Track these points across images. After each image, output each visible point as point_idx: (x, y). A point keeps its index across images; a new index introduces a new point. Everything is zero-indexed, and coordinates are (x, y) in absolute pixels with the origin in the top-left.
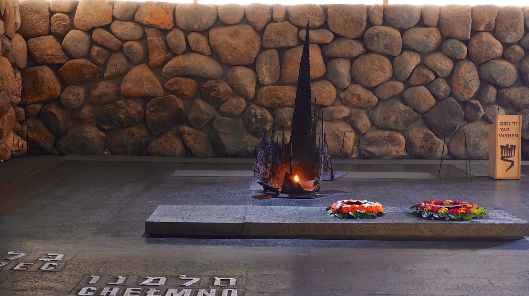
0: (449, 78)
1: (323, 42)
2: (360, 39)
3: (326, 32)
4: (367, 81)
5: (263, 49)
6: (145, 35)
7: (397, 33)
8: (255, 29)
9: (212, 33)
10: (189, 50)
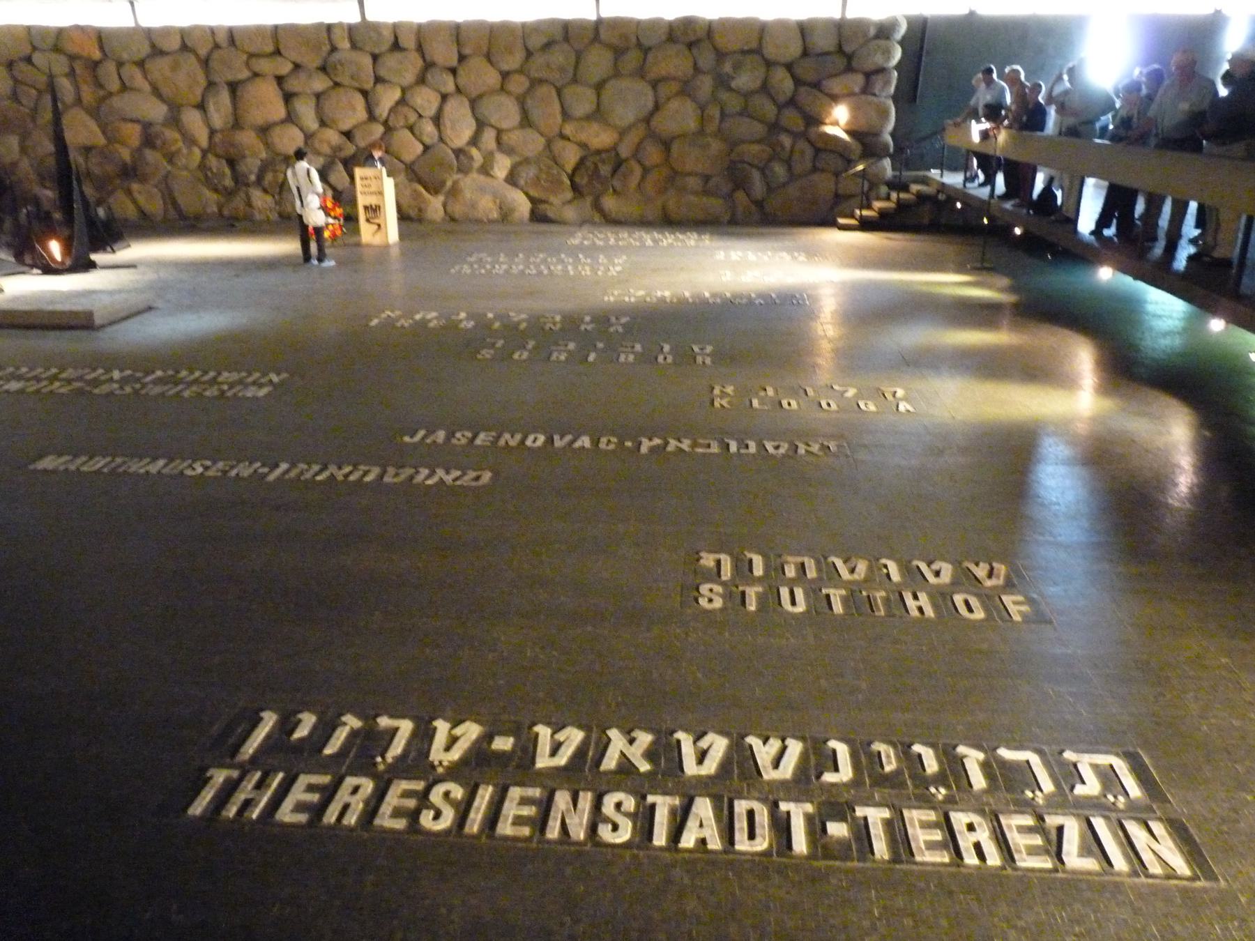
0: (437, 120)
2: (323, 69)
3: (279, 59)
5: (211, 84)
6: (73, 70)
7: (367, 61)
8: (197, 56)
10: (124, 88)
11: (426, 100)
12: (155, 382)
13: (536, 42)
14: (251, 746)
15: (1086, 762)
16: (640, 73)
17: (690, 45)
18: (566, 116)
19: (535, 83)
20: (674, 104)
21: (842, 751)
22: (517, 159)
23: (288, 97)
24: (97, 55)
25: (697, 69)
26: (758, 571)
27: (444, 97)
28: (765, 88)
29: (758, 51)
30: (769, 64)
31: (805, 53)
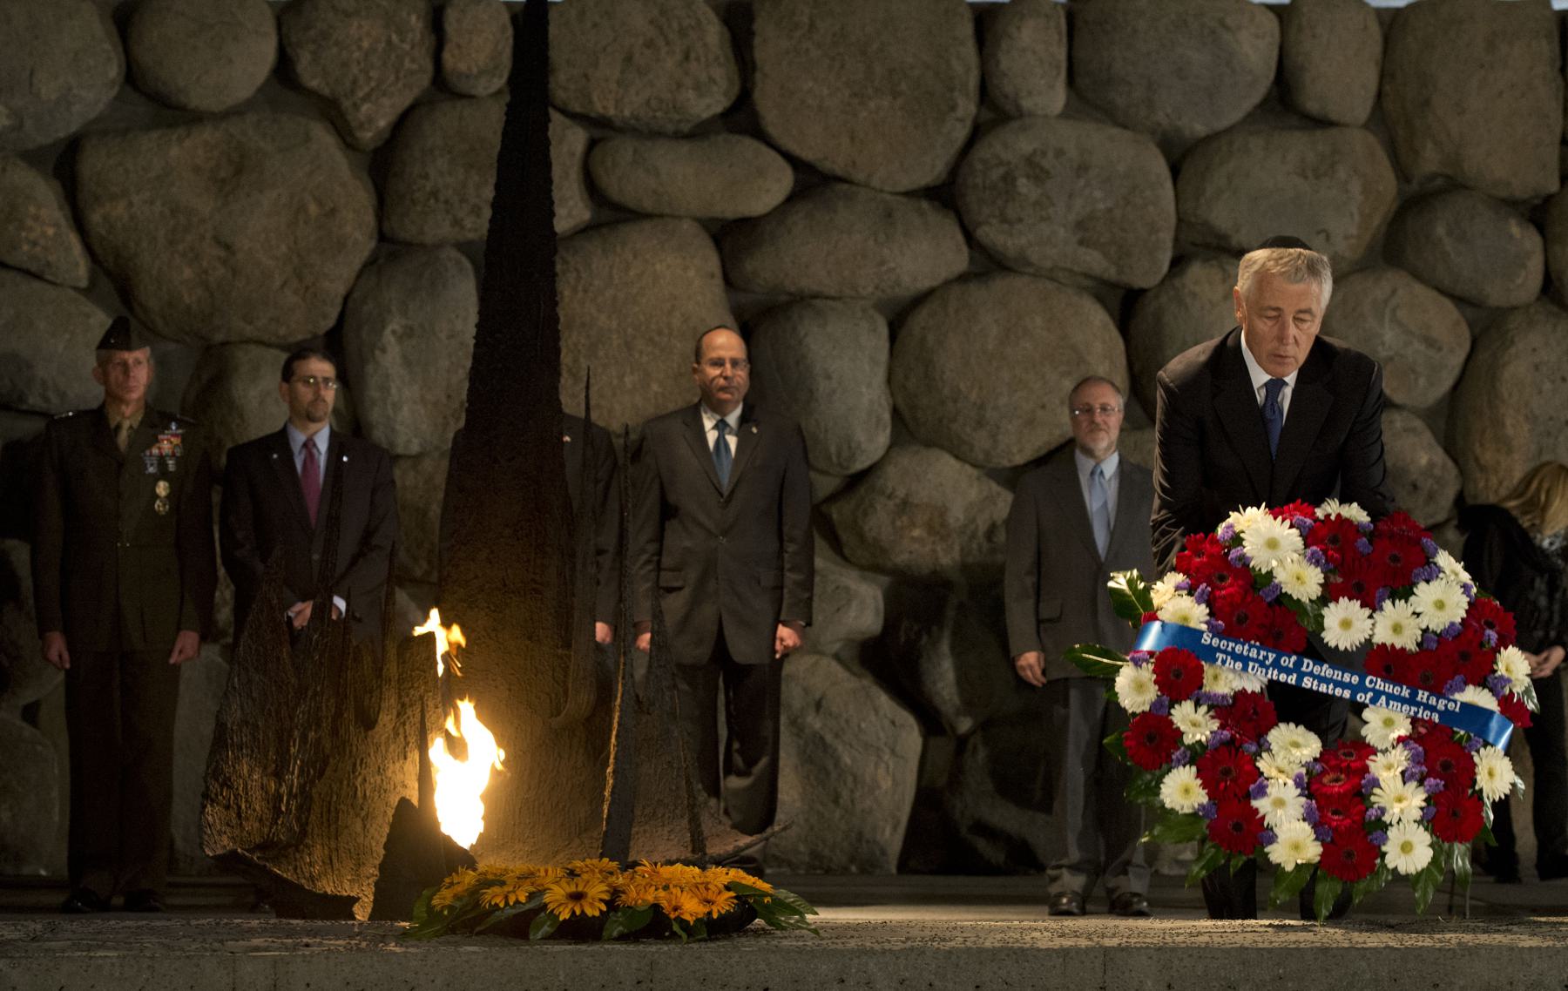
1: (730, 209)
2: (945, 195)
3: (749, 146)
4: (980, 423)
5: (391, 249)
9: (93, 163)
27: (1487, 328)
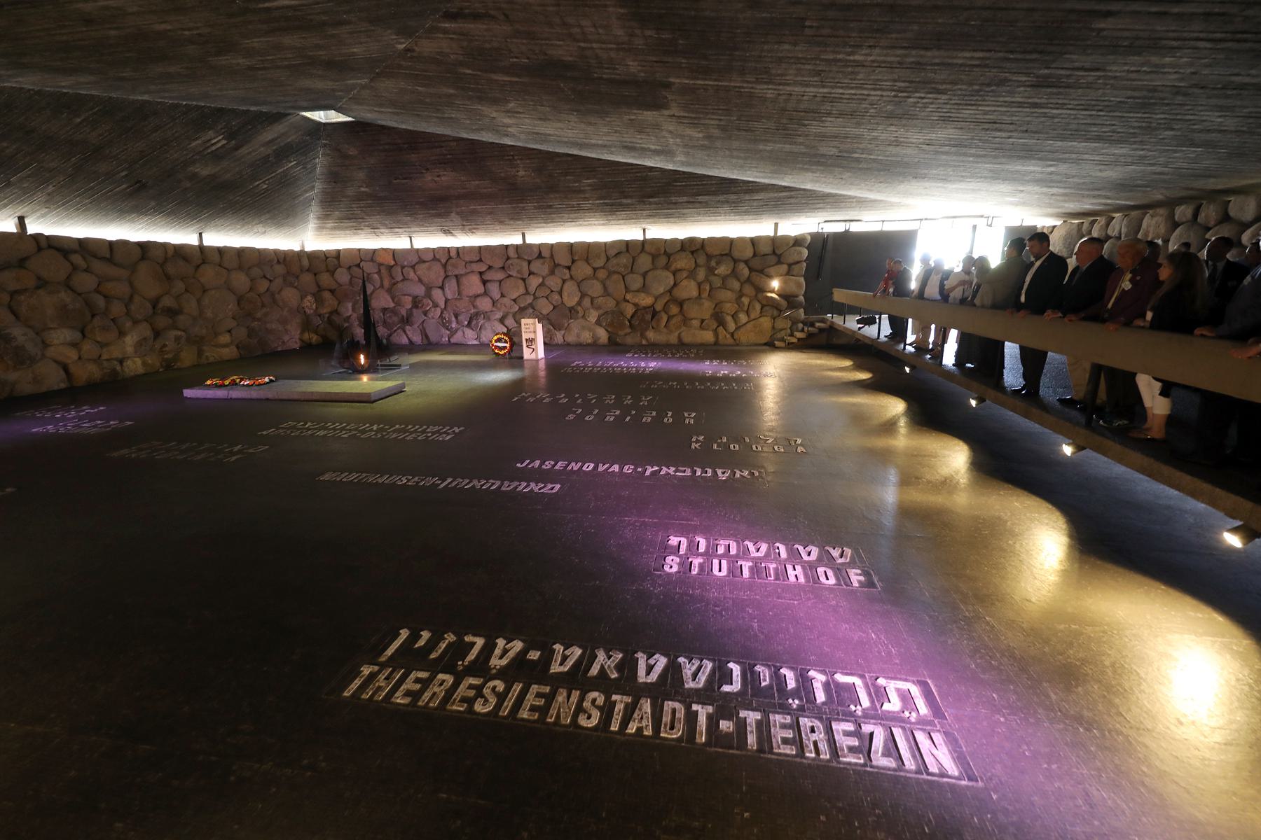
0: (560, 293)
5: (447, 276)
7: (525, 264)
10: (405, 279)
11: (554, 282)
12: (394, 431)
13: (612, 252)
14: (390, 651)
15: (893, 687)
16: (667, 267)
17: (692, 253)
18: (627, 290)
19: (610, 274)
20: (685, 283)
21: (736, 669)
22: (601, 312)
23: (484, 282)
24: (393, 263)
25: (697, 265)
26: (702, 549)
27: (564, 281)
28: (734, 274)
29: (729, 255)
30: (735, 261)
31: (755, 255)
